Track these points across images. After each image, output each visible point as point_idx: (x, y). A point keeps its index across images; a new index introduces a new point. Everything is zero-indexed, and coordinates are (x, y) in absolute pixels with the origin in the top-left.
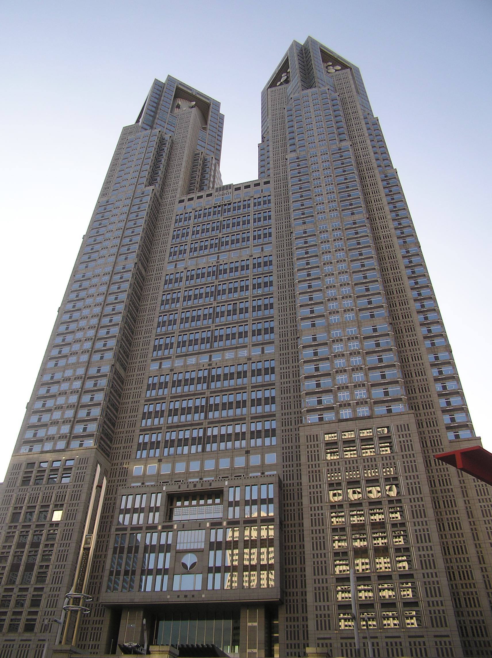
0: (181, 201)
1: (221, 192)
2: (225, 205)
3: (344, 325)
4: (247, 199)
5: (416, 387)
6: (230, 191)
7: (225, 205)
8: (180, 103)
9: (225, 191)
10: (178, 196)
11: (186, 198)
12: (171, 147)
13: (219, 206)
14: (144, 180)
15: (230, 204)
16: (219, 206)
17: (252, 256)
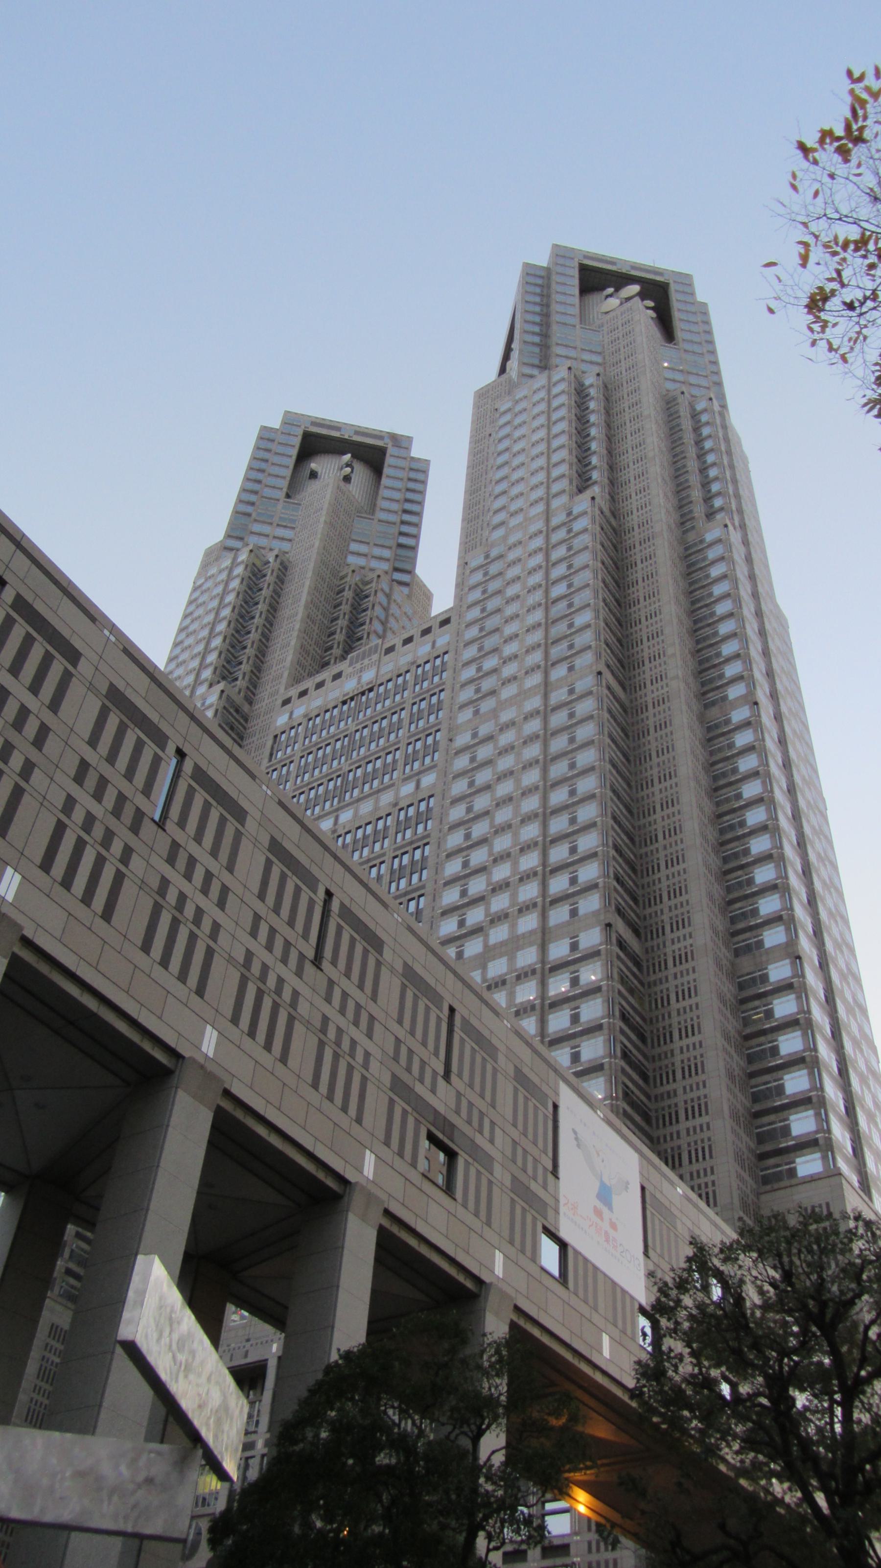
0: (287, 702)
1: (358, 666)
2: (363, 693)
3: (515, 944)
4: (403, 671)
5: (678, 1065)
6: (375, 657)
7: (363, 693)
8: (313, 465)
9: (366, 661)
10: (282, 690)
11: (294, 692)
12: (281, 580)
13: (352, 699)
14: (207, 674)
15: (371, 690)
16: (352, 699)
17: (396, 805)
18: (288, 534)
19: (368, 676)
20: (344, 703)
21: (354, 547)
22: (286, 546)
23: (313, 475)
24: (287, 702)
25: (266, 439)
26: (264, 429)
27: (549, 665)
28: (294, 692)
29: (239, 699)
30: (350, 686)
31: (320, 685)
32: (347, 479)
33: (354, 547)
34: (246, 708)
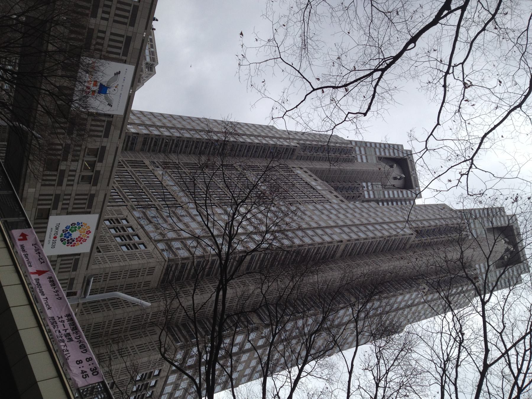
1: (322, 184)
13: (309, 184)
14: (302, 142)
18: (365, 161)
19: (319, 188)
20: (306, 183)
21: (369, 184)
22: (359, 160)
23: (392, 167)
24: (301, 168)
25: (398, 148)
26: (402, 146)
27: (340, 227)
28: (305, 169)
29: (296, 153)
30: (313, 183)
31: (311, 176)
32: (395, 178)
33: (369, 184)
34: (295, 157)
